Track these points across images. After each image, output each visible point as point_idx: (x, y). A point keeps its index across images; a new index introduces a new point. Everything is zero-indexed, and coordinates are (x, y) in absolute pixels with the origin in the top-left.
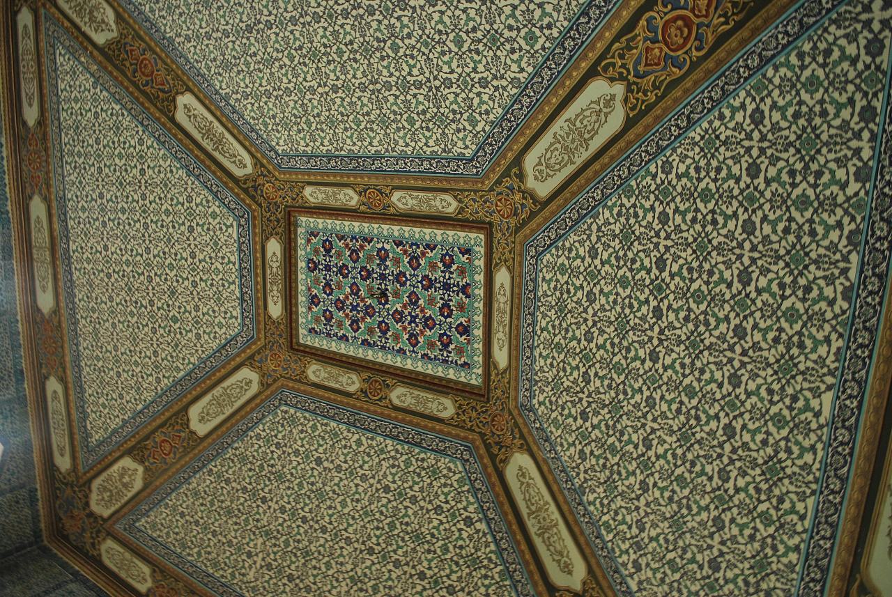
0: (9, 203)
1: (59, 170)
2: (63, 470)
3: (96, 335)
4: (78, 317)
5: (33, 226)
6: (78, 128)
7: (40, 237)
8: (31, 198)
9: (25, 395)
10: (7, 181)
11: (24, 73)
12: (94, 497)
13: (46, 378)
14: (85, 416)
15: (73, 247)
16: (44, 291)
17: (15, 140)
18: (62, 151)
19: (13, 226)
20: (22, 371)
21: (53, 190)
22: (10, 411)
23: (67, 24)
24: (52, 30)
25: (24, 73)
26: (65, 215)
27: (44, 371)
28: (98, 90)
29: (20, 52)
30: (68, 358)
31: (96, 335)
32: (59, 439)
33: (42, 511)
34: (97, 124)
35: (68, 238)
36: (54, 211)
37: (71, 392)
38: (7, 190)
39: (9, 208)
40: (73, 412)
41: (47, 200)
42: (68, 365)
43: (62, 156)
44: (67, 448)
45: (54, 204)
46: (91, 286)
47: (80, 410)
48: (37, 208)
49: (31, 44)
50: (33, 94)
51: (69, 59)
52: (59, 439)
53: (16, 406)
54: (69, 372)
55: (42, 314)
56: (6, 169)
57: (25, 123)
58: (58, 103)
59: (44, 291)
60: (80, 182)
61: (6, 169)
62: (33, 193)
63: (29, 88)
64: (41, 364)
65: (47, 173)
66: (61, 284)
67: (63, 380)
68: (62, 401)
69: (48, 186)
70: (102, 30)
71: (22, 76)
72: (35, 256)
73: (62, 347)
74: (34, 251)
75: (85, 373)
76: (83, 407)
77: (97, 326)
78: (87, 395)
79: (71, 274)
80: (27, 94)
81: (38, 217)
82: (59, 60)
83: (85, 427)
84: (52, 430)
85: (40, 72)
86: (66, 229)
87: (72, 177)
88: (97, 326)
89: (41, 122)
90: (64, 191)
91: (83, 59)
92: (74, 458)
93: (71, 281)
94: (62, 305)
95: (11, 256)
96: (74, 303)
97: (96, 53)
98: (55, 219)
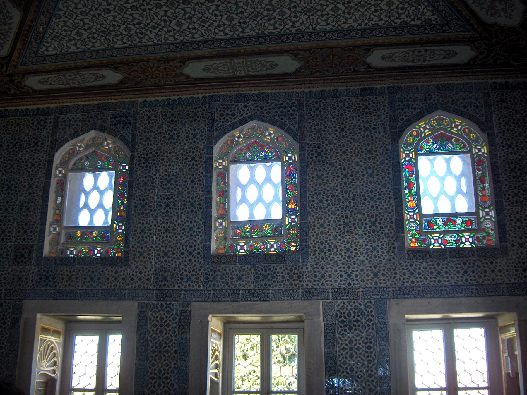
0: (196, 96)
1: (150, 48)
2: (473, 54)
3: (309, 11)
4: (294, 30)
5: (213, 75)
6: (103, 32)
7: (222, 68)
8: (188, 77)
9: (388, 88)
10: (176, 97)
11: (79, 83)
12: (502, 21)
13: (369, 66)
14: (404, 26)
15: (221, 35)
16: (276, 65)
17: (138, 91)
18: (130, 47)
19: (216, 92)
20: (363, 90)
21: (172, 55)
22: (402, 102)
23: (19, 46)
24: (31, 59)
25: (79, 83)
26: (192, 43)
27: (362, 68)
28: (61, 13)
29: (64, 86)
30: (343, 42)
31: (309, 11)
32: (437, 56)
33: (520, 80)
34: (92, 13)
35: (214, 41)
36: (192, 54)
37: (381, 40)
38: (183, 97)
39: (200, 96)
40: (402, 39)
41: (184, 61)
42: (350, 42)
43: (136, 46)
44: (446, 48)
45: (185, 54)
46: (256, 16)
47: (399, 31)
48: (195, 70)
49: (53, 77)
50: (94, 75)
51: (47, 42)
52: (437, 56)
53: (398, 96)
54: (358, 42)
55: (300, 68)
56: (165, 98)
57: (121, 82)
58: (89, 51)
59: (276, 65)
60: (154, 28)
61: (165, 98)
62: (184, 75)
63: (89, 78)
64: (355, 71)
65: (159, 61)
66: (263, 48)
67: (369, 48)
68: (392, 51)
69: (169, 60)
70: (9, 13)
71: (82, 85)
72: (243, 73)
73: (332, 48)
74: (238, 74)
75: (355, 25)
76: (395, 28)
77: (299, 9)
78: (380, 23)
79: (250, 37)
80: (95, 80)
81: (204, 70)
82: (52, 51)
83: (418, 27)
84: (427, 63)
85: (69, 69)
86: (205, 42)
87: (152, 36)
88: (299, 9)
89: (115, 67)
90: (169, 44)
91: (41, 29)
92: (457, 41)
93: (257, 37)
94: (285, 46)
95: (245, 95)
96: (280, 36)
97: (30, 17)
98: (199, 53)
